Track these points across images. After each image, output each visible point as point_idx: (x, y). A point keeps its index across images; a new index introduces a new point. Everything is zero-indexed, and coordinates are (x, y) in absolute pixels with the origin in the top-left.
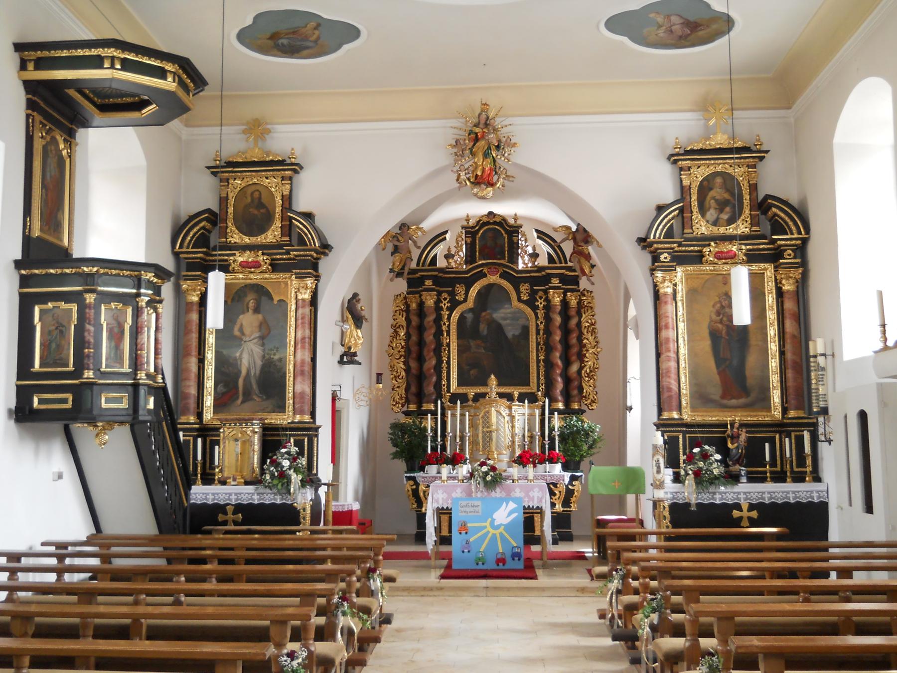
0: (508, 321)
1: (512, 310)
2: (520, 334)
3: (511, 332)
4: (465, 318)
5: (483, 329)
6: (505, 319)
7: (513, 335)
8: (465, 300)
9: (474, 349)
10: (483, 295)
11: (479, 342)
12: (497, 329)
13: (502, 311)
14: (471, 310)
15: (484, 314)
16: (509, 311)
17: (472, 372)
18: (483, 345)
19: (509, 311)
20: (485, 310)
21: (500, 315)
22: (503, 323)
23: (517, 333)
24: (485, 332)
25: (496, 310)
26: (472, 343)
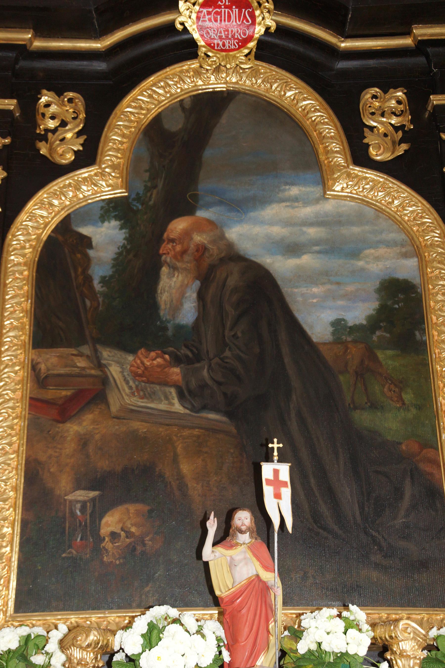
0: (306, 260)
1: (328, 207)
2: (374, 323)
3: (326, 309)
4: (86, 242)
5: (178, 295)
6: (293, 249)
7: (338, 325)
8: (87, 157)
9: (123, 395)
10: (181, 153)
11: (153, 360)
12: (253, 296)
13: (271, 211)
14: (113, 209)
15: (179, 225)
16: (307, 211)
17: (111, 522)
18: (176, 373)
19: (307, 211)
20: (188, 210)
21: (263, 229)
22: (280, 266)
23: (359, 313)
24: (188, 313)
25: (241, 207)
26: (118, 366)
